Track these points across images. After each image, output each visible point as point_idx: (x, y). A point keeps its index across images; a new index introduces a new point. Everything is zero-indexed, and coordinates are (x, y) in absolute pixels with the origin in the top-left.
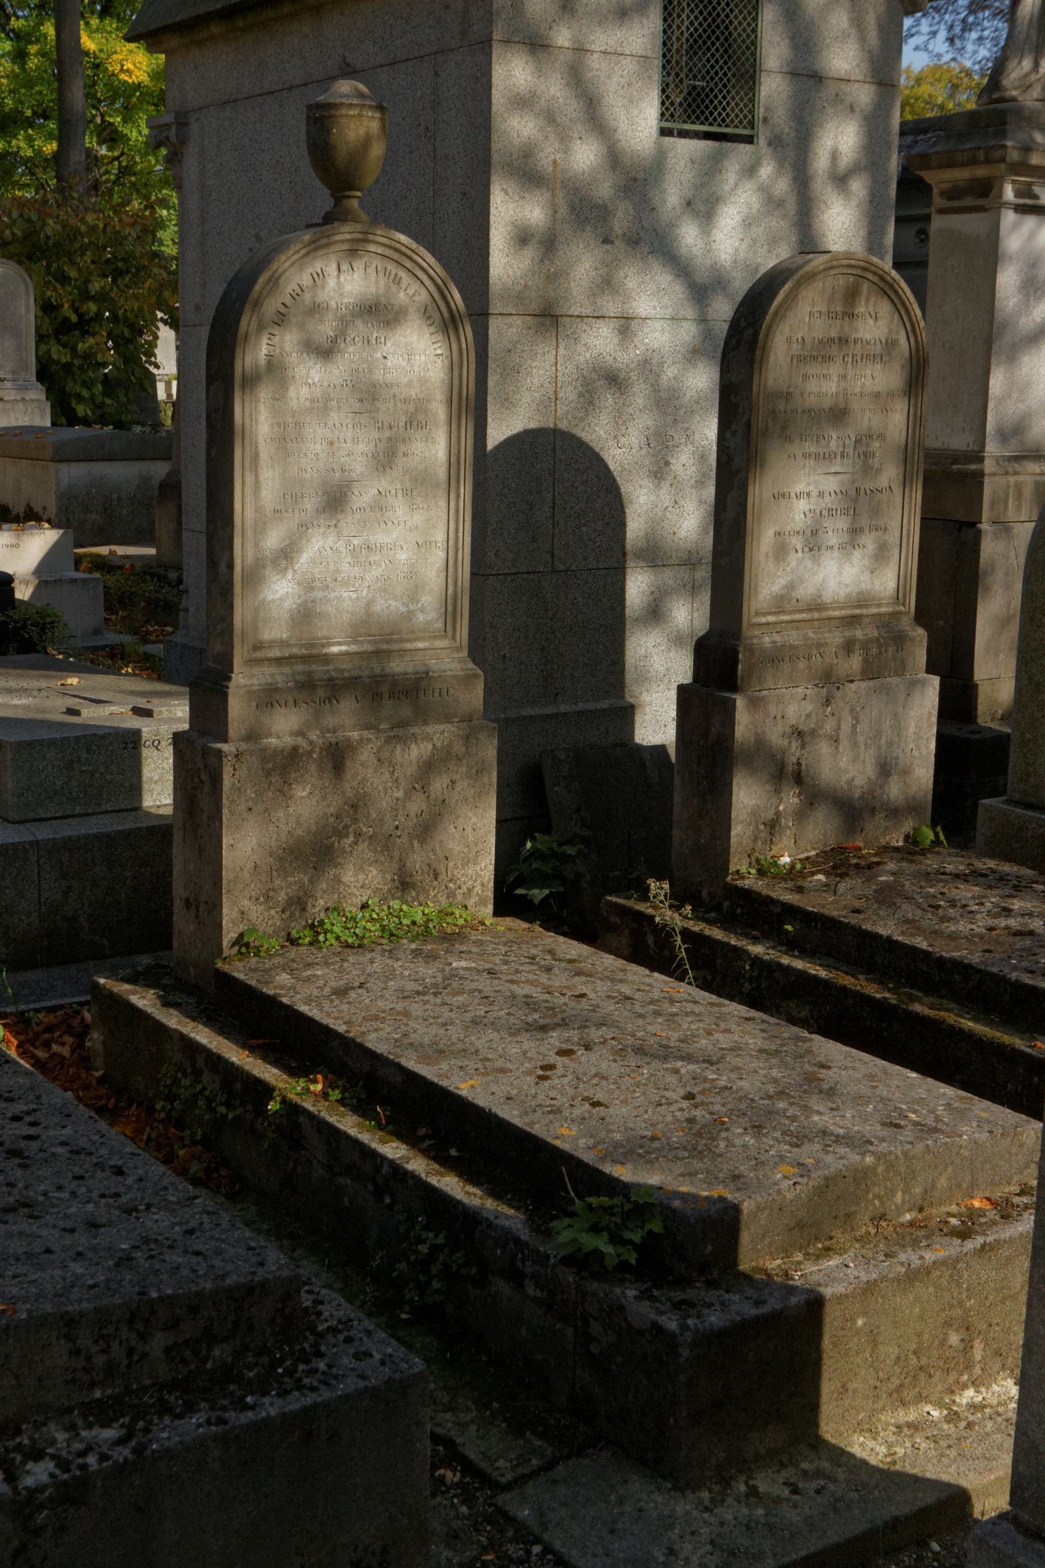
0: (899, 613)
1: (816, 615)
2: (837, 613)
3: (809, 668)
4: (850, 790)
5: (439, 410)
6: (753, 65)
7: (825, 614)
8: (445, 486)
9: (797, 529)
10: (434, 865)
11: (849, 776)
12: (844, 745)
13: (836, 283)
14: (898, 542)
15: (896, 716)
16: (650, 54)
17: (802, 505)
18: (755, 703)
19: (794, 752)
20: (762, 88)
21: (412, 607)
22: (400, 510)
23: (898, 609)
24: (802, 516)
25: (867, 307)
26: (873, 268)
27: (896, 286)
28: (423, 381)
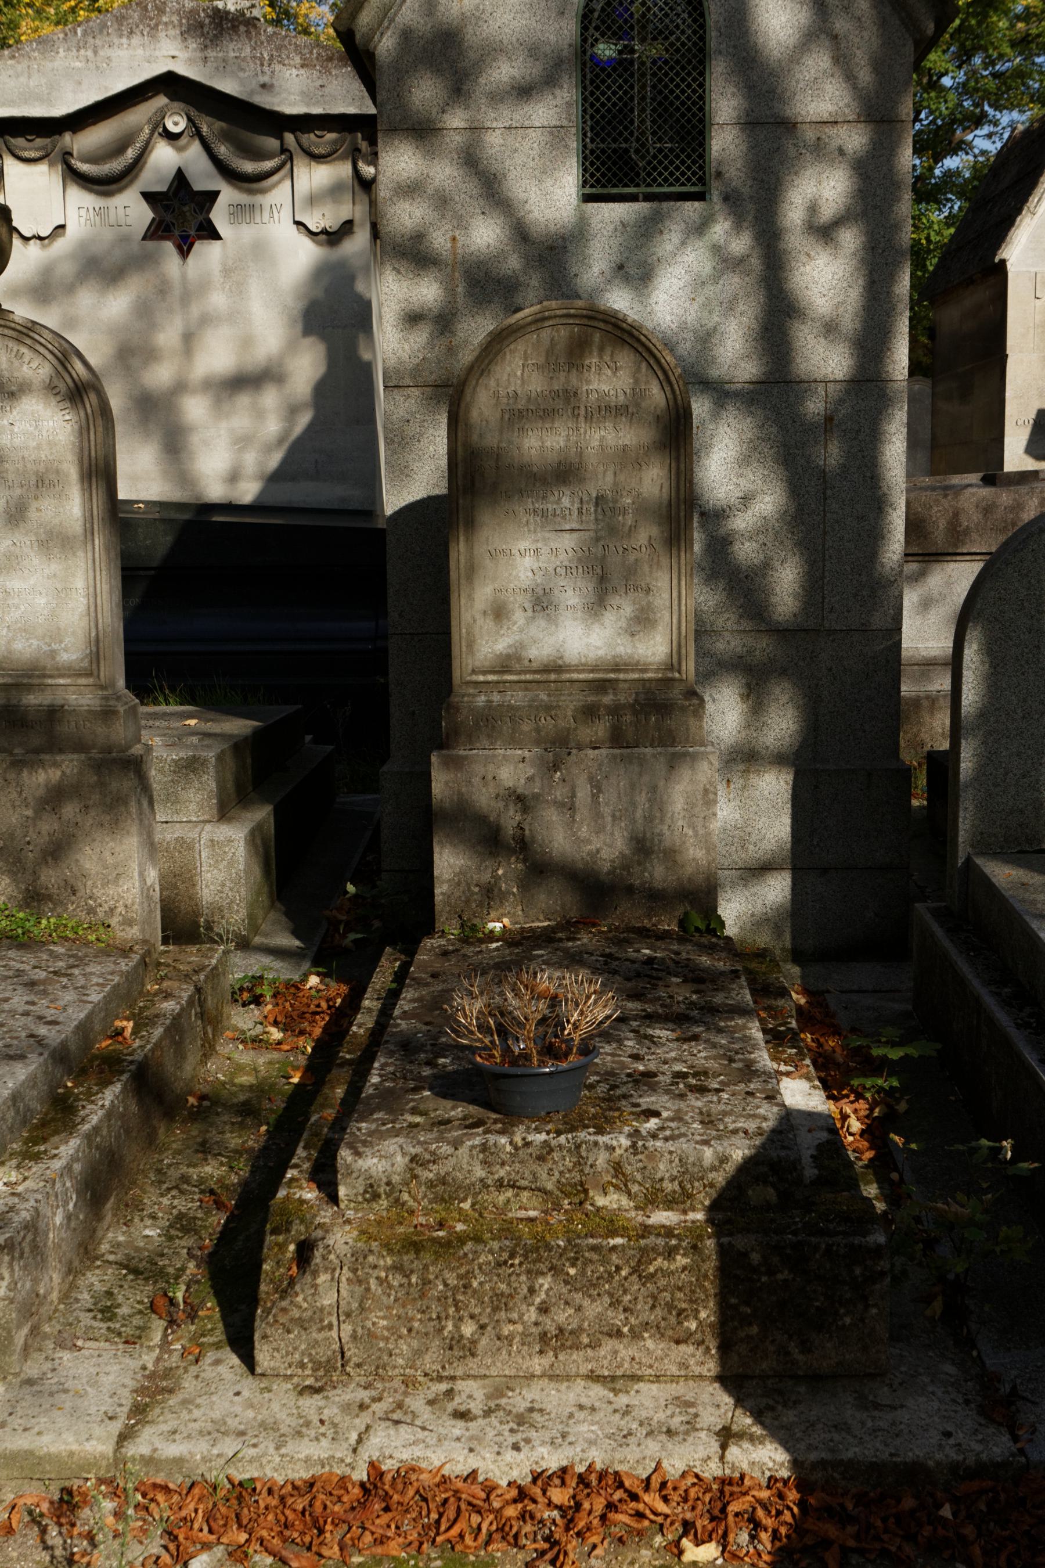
0: (673, 680)
1: (553, 677)
2: (582, 676)
3: (538, 730)
4: (595, 863)
5: (72, 472)
6: (702, 121)
7: (566, 676)
8: (82, 538)
9: (524, 587)
10: (72, 881)
11: (592, 848)
12: (583, 813)
13: (555, 334)
14: (668, 604)
15: (654, 789)
16: (565, 123)
17: (528, 561)
18: (455, 764)
19: (510, 819)
20: (714, 142)
21: (54, 646)
22: (35, 560)
23: (670, 675)
24: (530, 574)
25: (601, 357)
26: (601, 316)
27: (636, 333)
28: (51, 444)
